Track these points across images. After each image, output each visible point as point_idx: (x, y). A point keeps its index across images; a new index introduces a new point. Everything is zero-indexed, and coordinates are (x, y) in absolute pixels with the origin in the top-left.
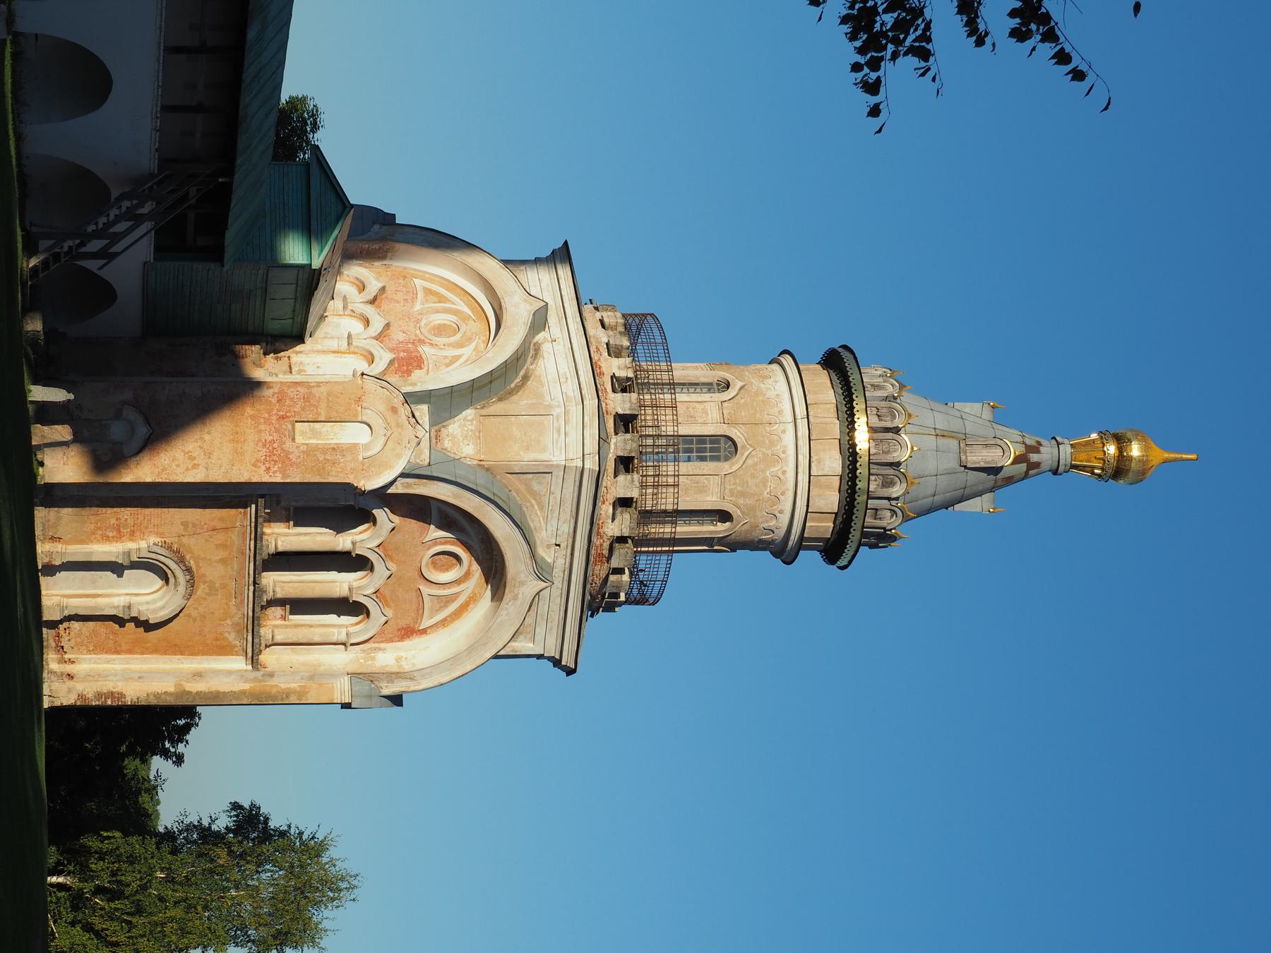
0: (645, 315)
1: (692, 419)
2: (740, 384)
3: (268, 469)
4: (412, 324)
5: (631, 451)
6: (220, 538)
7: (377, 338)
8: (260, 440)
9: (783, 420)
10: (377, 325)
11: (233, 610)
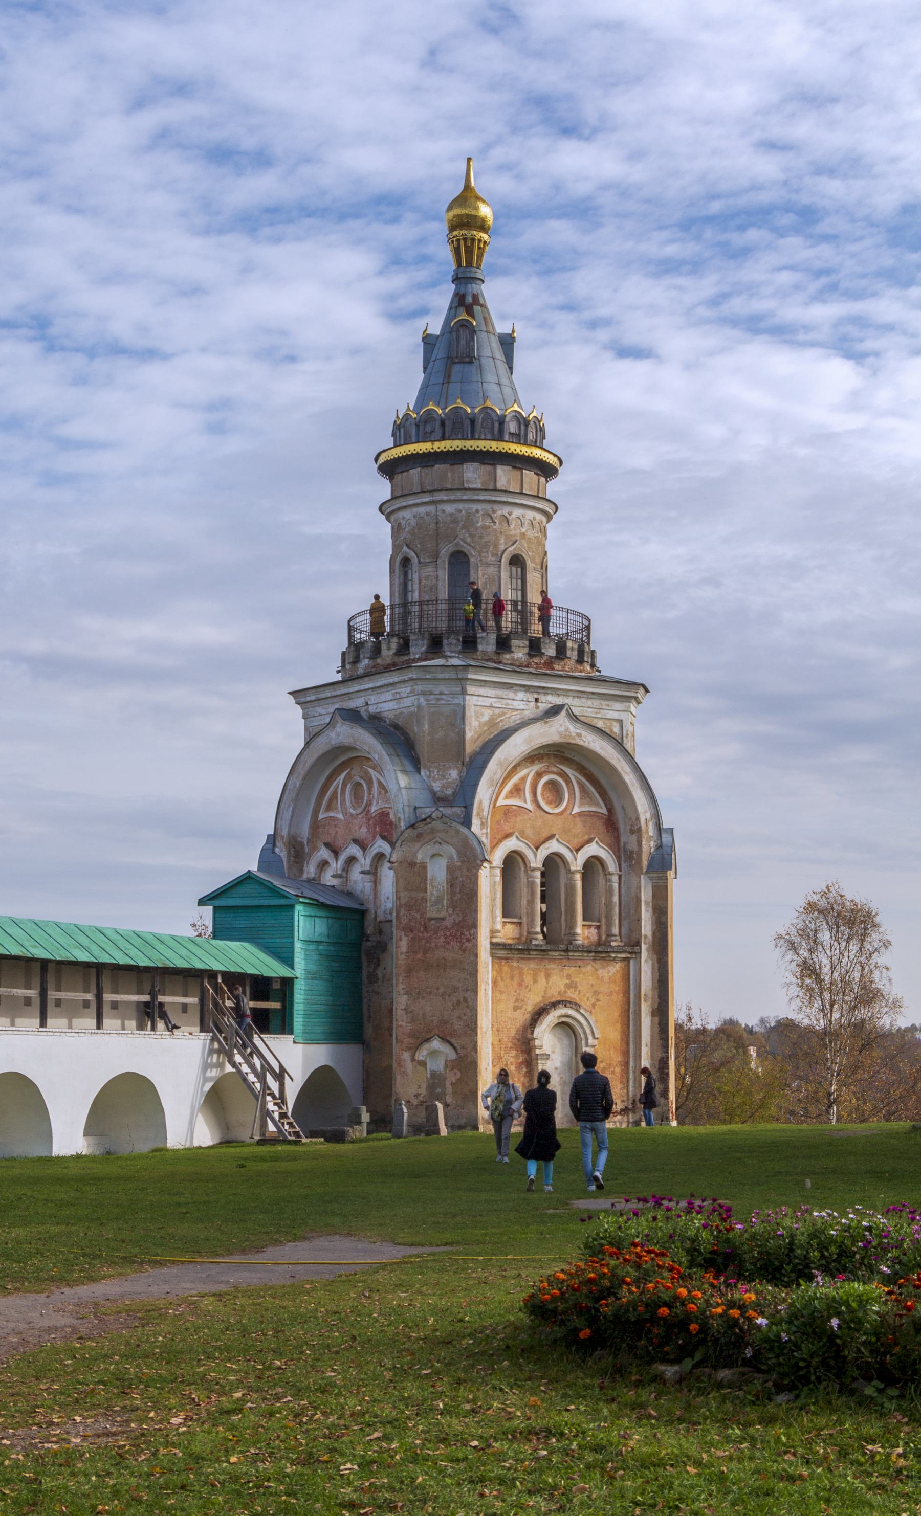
0: (350, 626)
1: (434, 589)
2: (405, 549)
3: (468, 940)
4: (354, 821)
5: (458, 640)
6: (528, 979)
8: (444, 947)
9: (433, 511)
10: (354, 850)
11: (589, 968)
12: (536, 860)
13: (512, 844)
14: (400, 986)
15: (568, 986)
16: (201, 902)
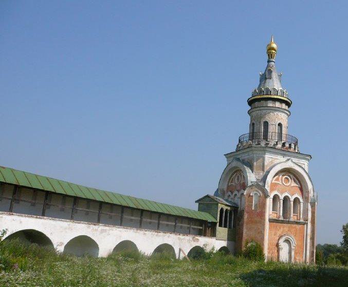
7: (239, 192)
10: (236, 192)
12: (282, 197)
13: (276, 192)
14: (244, 227)
16: (196, 202)
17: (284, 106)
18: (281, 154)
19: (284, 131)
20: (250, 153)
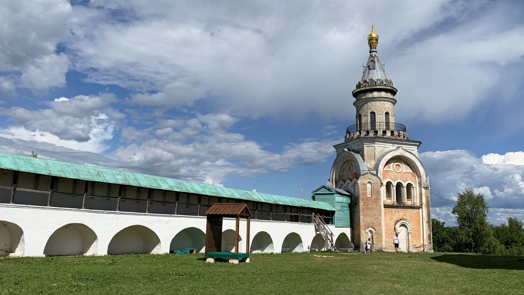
6: (394, 213)
10: (349, 181)
12: (395, 184)
13: (389, 180)
14: (361, 214)
15: (404, 215)
17: (389, 95)
18: (391, 143)
19: (392, 120)
20: (360, 143)
